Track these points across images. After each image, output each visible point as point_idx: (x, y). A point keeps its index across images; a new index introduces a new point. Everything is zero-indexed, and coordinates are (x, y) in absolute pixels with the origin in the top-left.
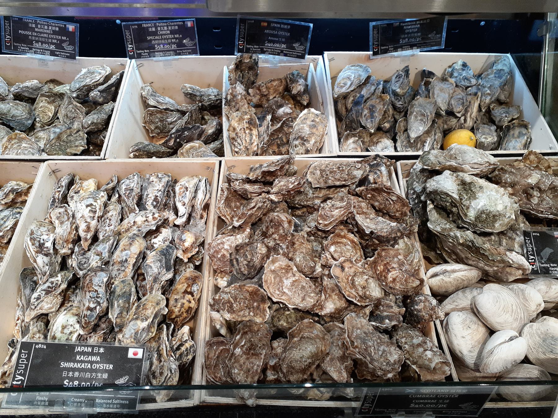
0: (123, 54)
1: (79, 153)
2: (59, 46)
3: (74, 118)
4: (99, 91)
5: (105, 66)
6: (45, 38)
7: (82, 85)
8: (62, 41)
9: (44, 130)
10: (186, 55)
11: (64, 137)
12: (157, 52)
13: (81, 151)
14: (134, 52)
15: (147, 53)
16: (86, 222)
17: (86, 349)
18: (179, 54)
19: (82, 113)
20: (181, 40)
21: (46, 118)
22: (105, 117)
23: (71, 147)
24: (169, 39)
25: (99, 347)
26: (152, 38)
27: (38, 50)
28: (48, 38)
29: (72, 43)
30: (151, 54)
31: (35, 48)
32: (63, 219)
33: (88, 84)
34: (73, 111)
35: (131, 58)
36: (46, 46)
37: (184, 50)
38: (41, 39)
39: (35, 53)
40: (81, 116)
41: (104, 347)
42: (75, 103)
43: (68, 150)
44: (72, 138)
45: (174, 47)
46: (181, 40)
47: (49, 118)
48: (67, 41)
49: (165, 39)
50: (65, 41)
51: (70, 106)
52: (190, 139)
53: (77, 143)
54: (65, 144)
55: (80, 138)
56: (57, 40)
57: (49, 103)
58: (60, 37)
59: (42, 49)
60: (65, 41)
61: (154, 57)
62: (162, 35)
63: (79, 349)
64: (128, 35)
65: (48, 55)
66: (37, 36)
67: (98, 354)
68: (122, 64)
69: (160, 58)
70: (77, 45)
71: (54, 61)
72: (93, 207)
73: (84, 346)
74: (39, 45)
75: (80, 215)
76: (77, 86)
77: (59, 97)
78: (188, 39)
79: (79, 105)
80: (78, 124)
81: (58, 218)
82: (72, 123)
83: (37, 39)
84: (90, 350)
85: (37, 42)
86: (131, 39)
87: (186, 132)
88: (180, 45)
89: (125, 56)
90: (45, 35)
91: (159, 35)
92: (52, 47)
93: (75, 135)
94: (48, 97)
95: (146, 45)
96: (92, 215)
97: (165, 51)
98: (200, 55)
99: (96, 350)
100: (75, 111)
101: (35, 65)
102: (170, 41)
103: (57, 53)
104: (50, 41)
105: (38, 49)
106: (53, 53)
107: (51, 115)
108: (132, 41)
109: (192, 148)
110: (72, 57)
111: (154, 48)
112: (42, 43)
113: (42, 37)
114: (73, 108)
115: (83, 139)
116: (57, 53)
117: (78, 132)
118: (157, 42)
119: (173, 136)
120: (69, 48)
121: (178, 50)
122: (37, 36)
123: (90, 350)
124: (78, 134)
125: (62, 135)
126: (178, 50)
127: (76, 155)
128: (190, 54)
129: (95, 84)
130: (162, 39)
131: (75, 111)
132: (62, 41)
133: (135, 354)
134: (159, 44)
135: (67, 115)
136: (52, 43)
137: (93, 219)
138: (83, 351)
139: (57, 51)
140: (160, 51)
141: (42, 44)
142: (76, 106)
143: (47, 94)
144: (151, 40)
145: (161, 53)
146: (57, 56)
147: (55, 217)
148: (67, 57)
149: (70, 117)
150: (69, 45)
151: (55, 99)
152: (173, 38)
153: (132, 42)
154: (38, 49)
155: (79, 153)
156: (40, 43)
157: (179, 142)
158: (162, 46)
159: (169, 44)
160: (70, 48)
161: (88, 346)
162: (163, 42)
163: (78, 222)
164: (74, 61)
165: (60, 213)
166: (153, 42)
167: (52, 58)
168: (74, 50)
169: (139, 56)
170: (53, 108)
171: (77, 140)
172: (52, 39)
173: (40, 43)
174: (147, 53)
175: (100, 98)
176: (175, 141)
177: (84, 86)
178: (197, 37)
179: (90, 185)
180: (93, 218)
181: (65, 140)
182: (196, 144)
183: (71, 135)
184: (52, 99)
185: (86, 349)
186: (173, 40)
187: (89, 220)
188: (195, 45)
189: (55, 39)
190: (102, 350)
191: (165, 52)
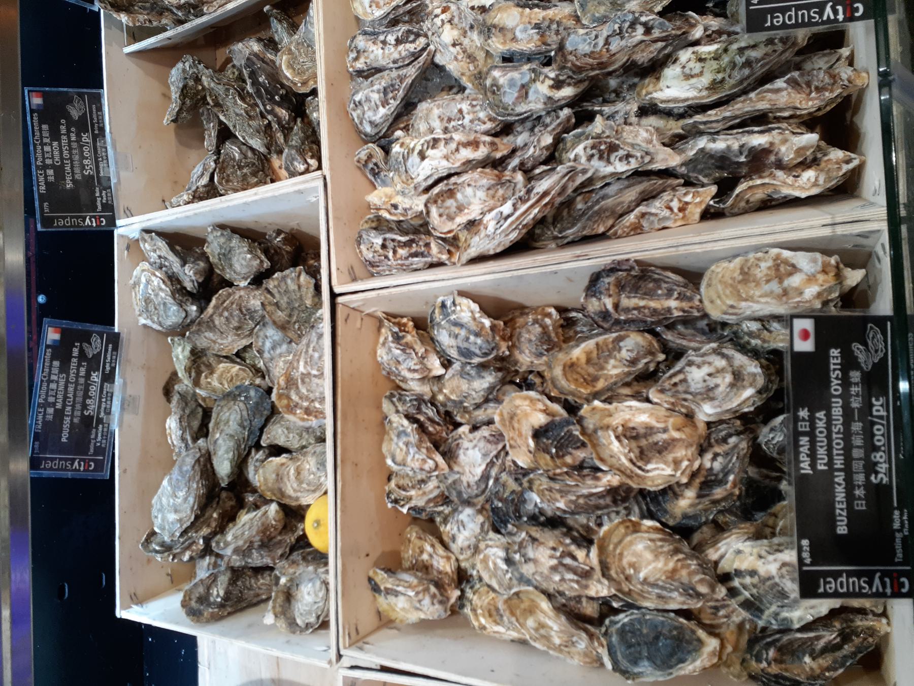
0: (105, 239)
1: (313, 281)
2: (93, 363)
3: (241, 310)
4: (183, 265)
5: (132, 282)
6: (76, 389)
7: (172, 301)
8: (82, 355)
9: (268, 371)
10: (103, 116)
11: (281, 315)
12: (98, 172)
13: (308, 278)
14: (102, 217)
15: (101, 193)
16: (457, 150)
17: (805, 450)
18: (102, 130)
19: (229, 295)
20: (70, 122)
21: (242, 373)
22: (235, 241)
23: (301, 298)
24: (69, 146)
25: (796, 419)
26: (68, 179)
27: (103, 405)
28: (77, 383)
29: (86, 337)
30: (105, 184)
31: (99, 413)
32: (453, 209)
33: (169, 293)
34: (226, 314)
35: (112, 222)
36: (94, 390)
37: (92, 119)
38: (79, 399)
39: (108, 412)
40: (237, 297)
41: (796, 410)
42: (210, 310)
43: (308, 302)
44: (283, 302)
45: (86, 138)
46: (70, 122)
47: (244, 370)
48: (81, 346)
49: (71, 154)
50: (82, 351)
51: (217, 322)
52: (275, 75)
53: (292, 286)
54: (296, 313)
55: (283, 284)
56: (79, 365)
57: (212, 373)
58: (74, 360)
59: (100, 398)
60: (82, 351)
61: (109, 179)
62: (62, 158)
63: (806, 467)
64: (65, 222)
65: (112, 388)
66: (73, 406)
67: (812, 420)
68: (128, 248)
69: (112, 169)
70: (88, 326)
71: (122, 376)
72: (425, 147)
73: (797, 453)
74: (92, 404)
75: (445, 163)
76: (175, 308)
77: (200, 357)
78: (69, 108)
79: (214, 302)
80: (254, 297)
81: (451, 218)
82: (251, 313)
83: (78, 406)
84: (804, 440)
85: (85, 407)
86: (72, 217)
87: (261, 80)
88: (82, 125)
89: (111, 234)
90: (71, 389)
91: (63, 163)
92: (96, 377)
93: (277, 295)
94: (199, 374)
95: (84, 197)
96: (442, 143)
97: (96, 158)
98: (102, 88)
99: (804, 427)
100: (226, 309)
101: (134, 421)
102: (74, 145)
103: (108, 368)
104: (82, 381)
105: (99, 407)
106: (109, 378)
107: (238, 367)
108: (77, 217)
109: (290, 66)
110: (115, 340)
111: (91, 177)
112: (86, 396)
113: (75, 396)
114: (221, 315)
115: (284, 278)
116: (108, 368)
117: (269, 292)
118: (77, 170)
119: (268, 107)
120: (96, 345)
121: (93, 130)
122: (73, 406)
123: (804, 440)
124: (275, 291)
125: (277, 320)
126: (93, 130)
127: (318, 288)
128: (100, 109)
129: (169, 283)
130: (71, 159)
131: (226, 309)
132: (82, 355)
133: (805, 335)
134: (83, 167)
135: (238, 328)
136: (88, 376)
137: (451, 138)
138: (808, 456)
139: (104, 368)
140: (97, 167)
141: (90, 398)
142: (216, 307)
143: (193, 374)
144: (74, 181)
145: (101, 165)
146: (113, 370)
147: (450, 223)
148: (116, 348)
149: (240, 321)
150: (90, 344)
151: (204, 364)
152: (69, 137)
153: (80, 217)
154: (99, 407)
155: (313, 281)
156: (88, 401)
157: (281, 97)
158: (86, 162)
159: (81, 147)
160: (96, 341)
161: (797, 445)
162: (77, 158)
163: (458, 164)
164: (124, 336)
165: (441, 215)
166: (78, 177)
167: (118, 380)
168: (101, 335)
169: (109, 207)
170: (222, 365)
171: (287, 291)
172: (77, 375)
173: (88, 401)
174: (101, 193)
175: (198, 265)
176: (279, 105)
177: (174, 299)
178: (65, 89)
179: (376, 197)
180: (447, 141)
181: (287, 312)
182: (282, 61)
183: (277, 305)
184: (203, 368)
185: (805, 450)
186: (73, 138)
187: (453, 146)
188: (81, 95)
189: (78, 370)
190: (803, 413)
191: (98, 157)
